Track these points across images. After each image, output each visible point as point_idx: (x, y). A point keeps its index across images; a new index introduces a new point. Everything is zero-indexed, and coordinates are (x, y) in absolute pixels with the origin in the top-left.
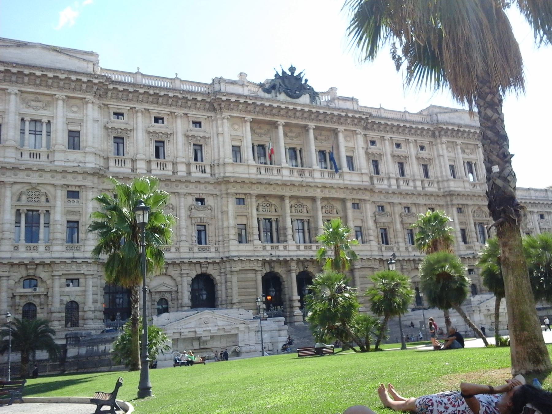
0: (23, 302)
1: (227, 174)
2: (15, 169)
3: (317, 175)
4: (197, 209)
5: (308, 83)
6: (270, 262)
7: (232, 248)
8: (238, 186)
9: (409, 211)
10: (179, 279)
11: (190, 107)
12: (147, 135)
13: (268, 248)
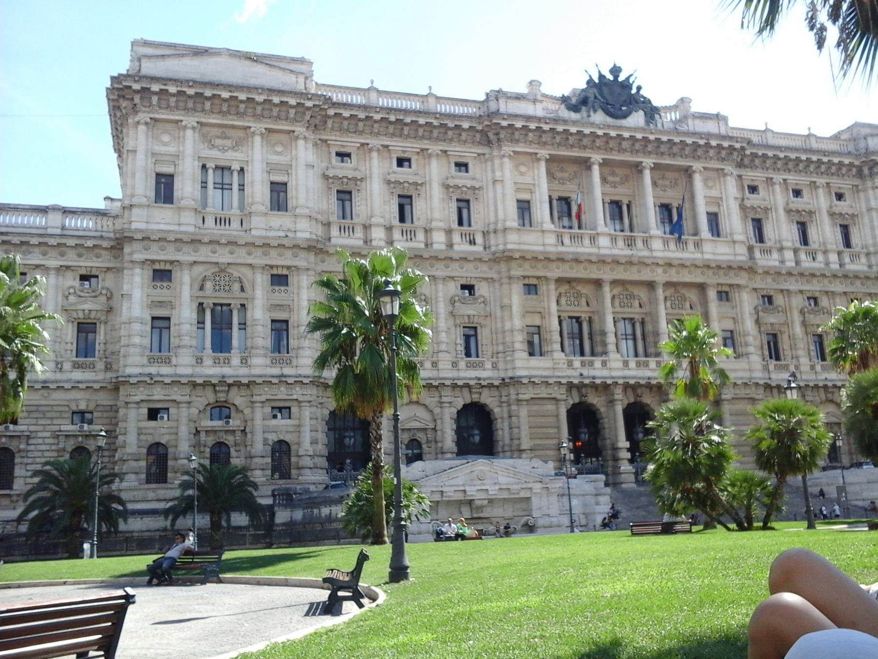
0: (211, 440)
1: (509, 246)
2: (195, 242)
3: (657, 245)
4: (463, 301)
5: (641, 92)
6: (580, 387)
7: (518, 364)
8: (527, 265)
9: (816, 304)
10: (437, 410)
11: (451, 140)
12: (386, 187)
13: (577, 364)
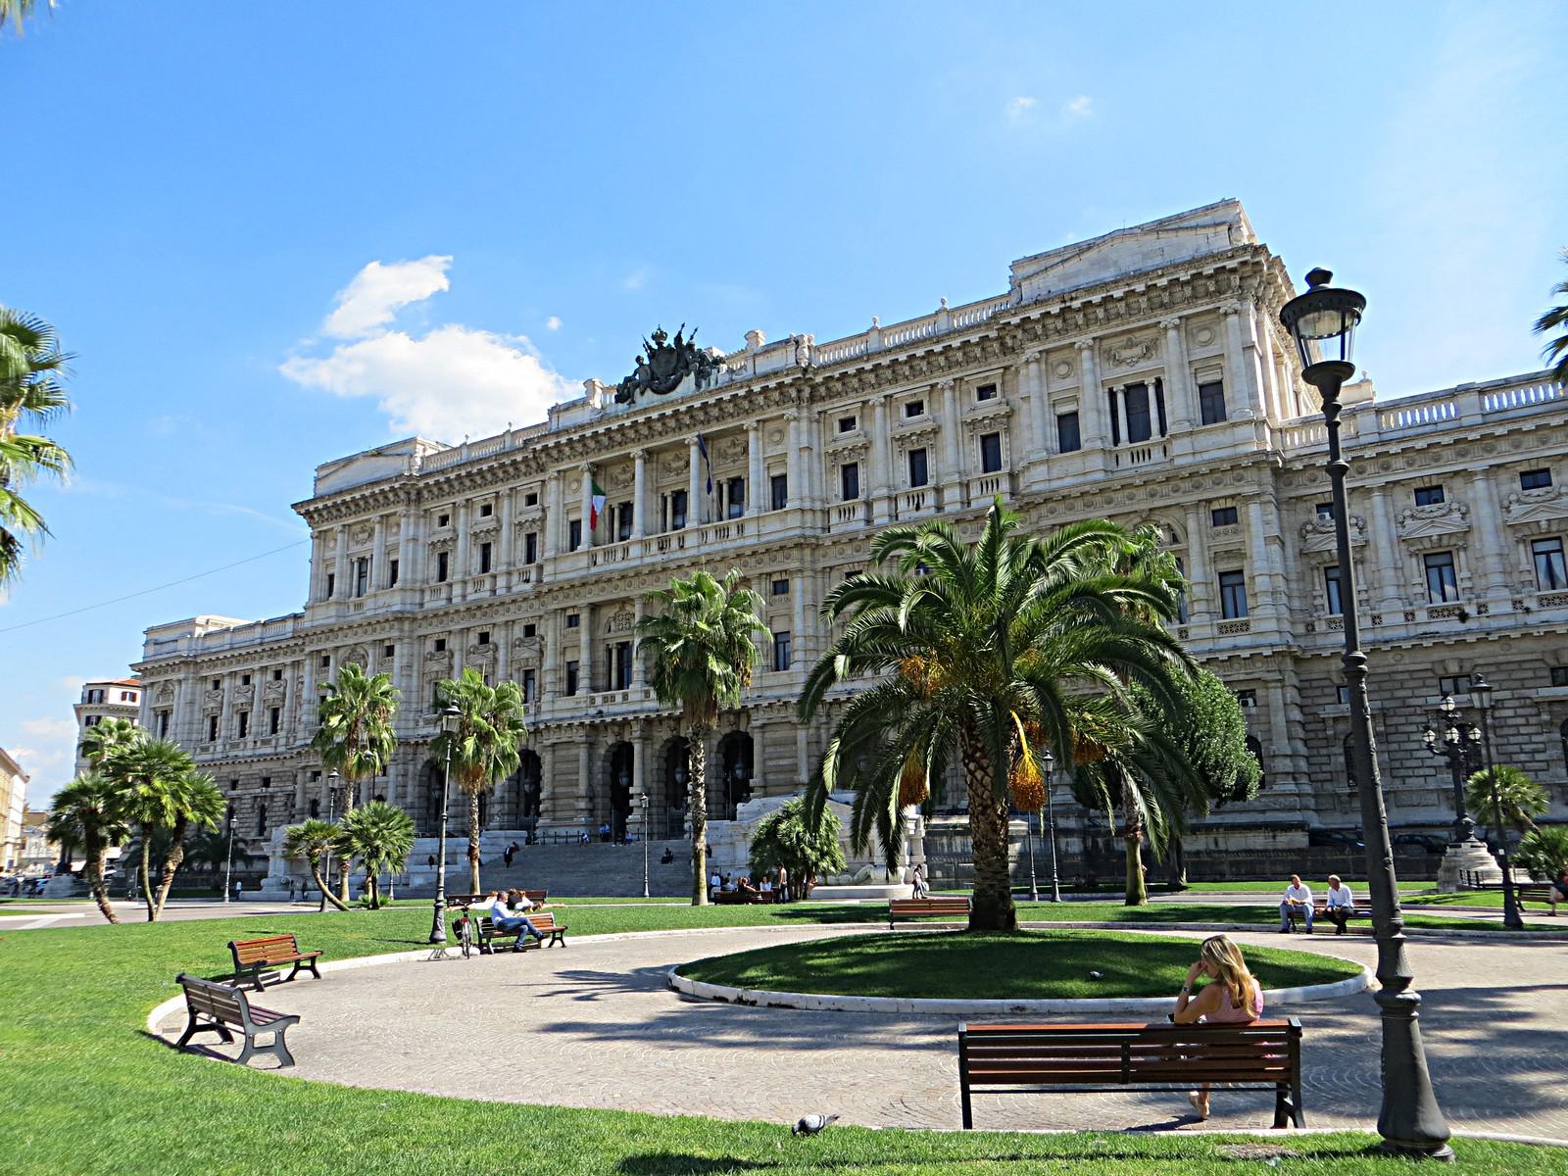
3: (691, 541)
